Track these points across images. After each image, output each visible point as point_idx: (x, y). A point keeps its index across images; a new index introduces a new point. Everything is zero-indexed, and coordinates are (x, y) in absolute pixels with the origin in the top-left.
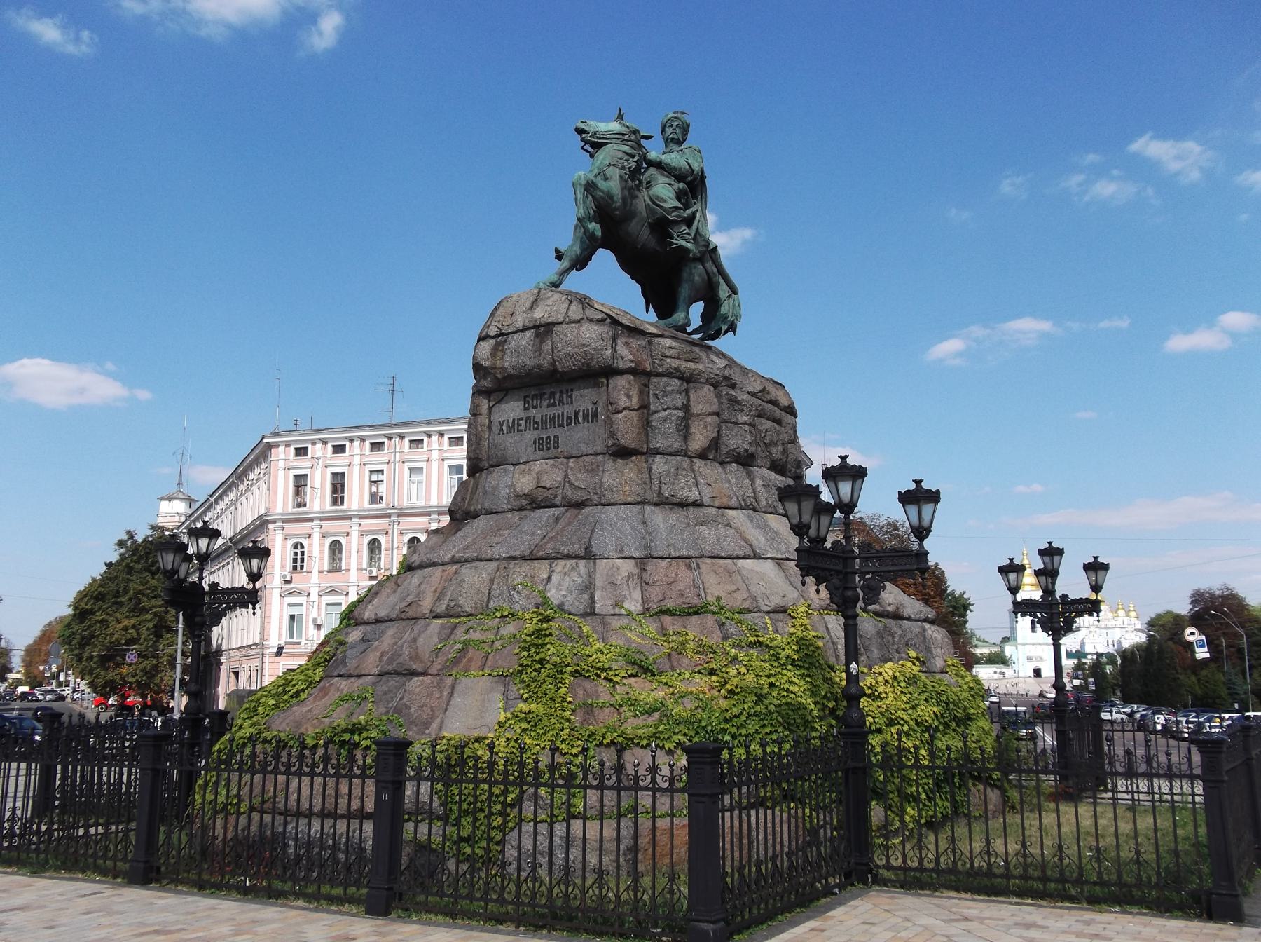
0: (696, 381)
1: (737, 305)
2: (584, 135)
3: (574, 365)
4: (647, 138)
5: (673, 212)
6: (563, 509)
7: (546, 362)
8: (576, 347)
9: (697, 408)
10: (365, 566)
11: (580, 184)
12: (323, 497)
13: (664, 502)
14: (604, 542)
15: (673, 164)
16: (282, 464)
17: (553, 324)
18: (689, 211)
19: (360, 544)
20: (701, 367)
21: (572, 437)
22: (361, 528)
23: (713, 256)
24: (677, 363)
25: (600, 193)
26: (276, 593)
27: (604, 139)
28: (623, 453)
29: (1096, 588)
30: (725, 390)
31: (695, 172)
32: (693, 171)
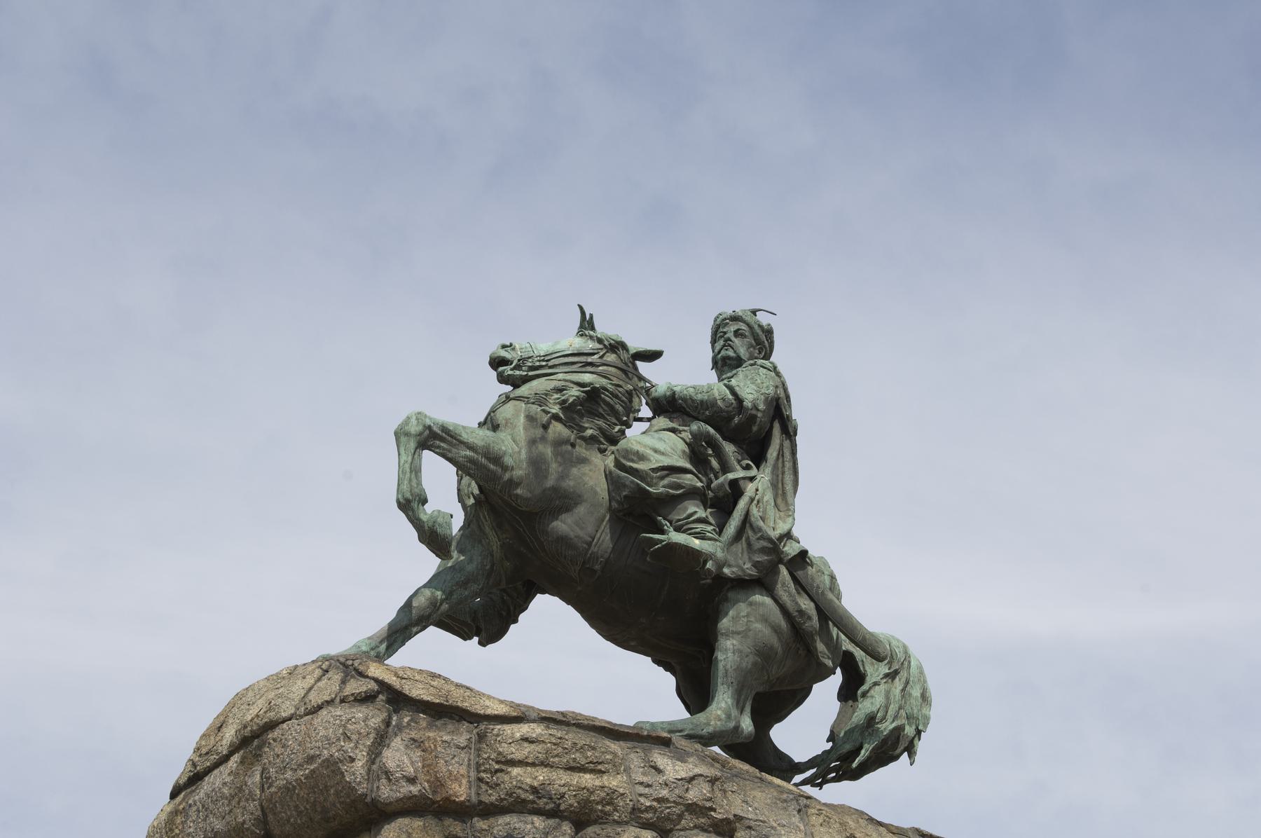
0: (602, 819)
1: (916, 692)
2: (501, 369)
3: (300, 813)
4: (652, 356)
5: (662, 478)
8: (300, 766)
11: (407, 434)
15: (699, 397)
17: (272, 725)
20: (614, 782)
23: (799, 574)
24: (541, 775)
25: (468, 453)
27: (541, 367)
31: (748, 404)
32: (740, 401)
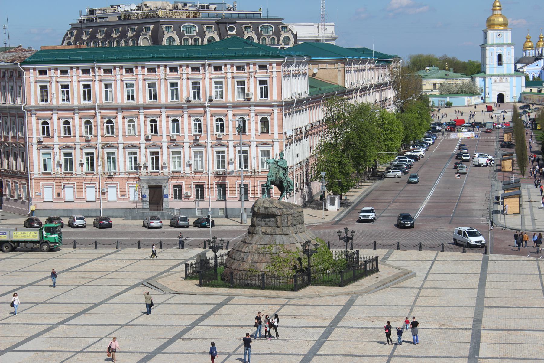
6: (269, 236)
7: (267, 213)
9: (289, 219)
10: (84, 134)
12: (57, 98)
13: (284, 234)
14: (277, 243)
16: (32, 79)
18: (285, 176)
19: (80, 123)
21: (270, 224)
22: (80, 114)
26: (35, 147)
28: (278, 227)
29: (353, 236)
30: (293, 215)
